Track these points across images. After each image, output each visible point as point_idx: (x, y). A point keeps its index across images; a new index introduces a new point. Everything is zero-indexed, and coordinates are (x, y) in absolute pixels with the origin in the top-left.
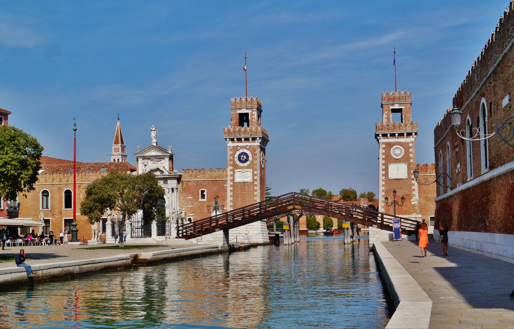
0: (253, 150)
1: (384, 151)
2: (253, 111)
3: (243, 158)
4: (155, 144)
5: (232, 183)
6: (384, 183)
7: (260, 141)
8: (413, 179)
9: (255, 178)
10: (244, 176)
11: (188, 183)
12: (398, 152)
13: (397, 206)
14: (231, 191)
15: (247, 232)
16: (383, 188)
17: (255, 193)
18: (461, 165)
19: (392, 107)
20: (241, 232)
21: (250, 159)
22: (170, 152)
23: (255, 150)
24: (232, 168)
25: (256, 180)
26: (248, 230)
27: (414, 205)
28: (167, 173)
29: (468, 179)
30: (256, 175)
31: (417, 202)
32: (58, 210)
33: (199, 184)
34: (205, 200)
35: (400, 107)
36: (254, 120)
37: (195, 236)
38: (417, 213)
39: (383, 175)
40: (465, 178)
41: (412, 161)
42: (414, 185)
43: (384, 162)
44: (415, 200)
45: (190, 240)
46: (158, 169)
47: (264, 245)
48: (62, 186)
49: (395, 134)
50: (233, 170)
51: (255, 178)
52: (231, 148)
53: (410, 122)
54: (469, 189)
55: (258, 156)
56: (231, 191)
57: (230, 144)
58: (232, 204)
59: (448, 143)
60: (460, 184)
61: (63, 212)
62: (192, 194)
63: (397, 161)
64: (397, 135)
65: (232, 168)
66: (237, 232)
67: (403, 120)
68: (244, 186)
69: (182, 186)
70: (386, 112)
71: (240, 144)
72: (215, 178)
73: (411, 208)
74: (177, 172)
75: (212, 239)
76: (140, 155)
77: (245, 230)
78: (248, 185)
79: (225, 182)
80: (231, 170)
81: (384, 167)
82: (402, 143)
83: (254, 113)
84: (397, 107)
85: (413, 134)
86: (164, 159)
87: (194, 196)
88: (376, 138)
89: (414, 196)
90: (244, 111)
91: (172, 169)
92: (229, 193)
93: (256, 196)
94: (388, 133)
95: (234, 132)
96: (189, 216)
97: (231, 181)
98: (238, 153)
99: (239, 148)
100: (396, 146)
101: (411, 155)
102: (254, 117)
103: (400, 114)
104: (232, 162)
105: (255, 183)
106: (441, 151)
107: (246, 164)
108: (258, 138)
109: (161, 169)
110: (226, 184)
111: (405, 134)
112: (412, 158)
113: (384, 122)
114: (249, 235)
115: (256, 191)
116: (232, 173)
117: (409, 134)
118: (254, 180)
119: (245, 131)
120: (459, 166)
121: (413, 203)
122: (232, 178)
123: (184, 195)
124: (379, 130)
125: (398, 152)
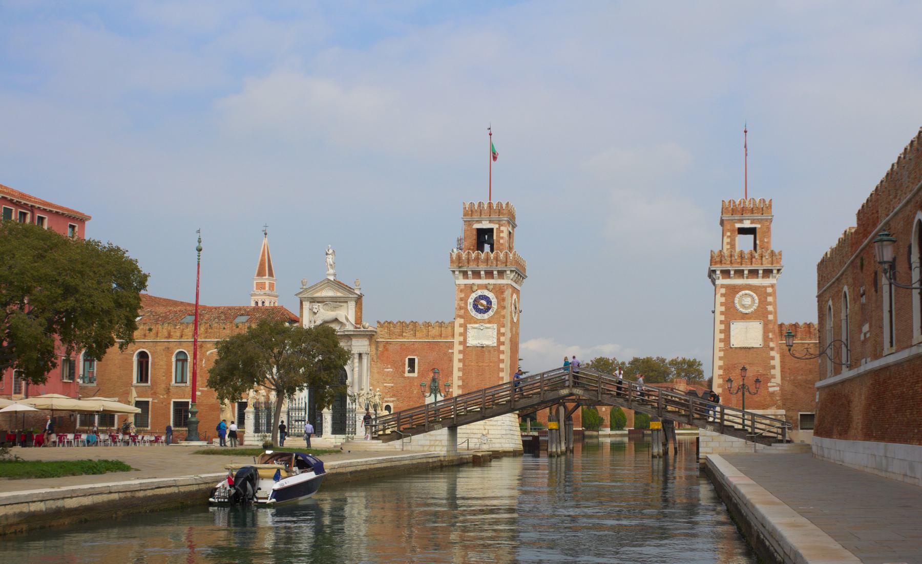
0: (499, 291)
1: (723, 300)
2: (500, 225)
3: (482, 305)
4: (332, 278)
5: (461, 348)
6: (722, 354)
7: (512, 276)
8: (772, 349)
9: (502, 339)
10: (482, 335)
12: (747, 301)
13: (747, 394)
14: (460, 360)
16: (721, 363)
17: (501, 366)
18: (870, 327)
19: (738, 225)
20: (475, 431)
21: (495, 306)
22: (358, 292)
23: (502, 293)
24: (462, 321)
25: (503, 343)
26: (487, 427)
27: (773, 393)
28: (352, 328)
29: (886, 352)
30: (503, 334)
31: (778, 389)
33: (405, 348)
34: (415, 375)
35: (753, 226)
36: (501, 241)
37: (399, 437)
38: (779, 408)
39: (721, 340)
40: (879, 349)
41: (771, 317)
42: (773, 358)
43: (723, 318)
44: (775, 385)
45: (391, 443)
46: (336, 320)
47: (514, 454)
48: (171, 345)
49: (743, 271)
50: (464, 326)
51: (502, 339)
52: (462, 287)
53: (769, 251)
54: (886, 368)
55: (507, 303)
56: (460, 360)
57: (461, 281)
58: (460, 383)
59: (846, 288)
60: (869, 359)
61: (172, 390)
62: (394, 364)
63: (745, 317)
64: (746, 272)
65: (462, 321)
66: (469, 431)
67: (758, 248)
68: (483, 352)
69: (377, 350)
70: (729, 234)
71: (477, 282)
73: (769, 399)
74: (369, 324)
75: (428, 443)
76: (305, 296)
77: (482, 427)
78: (489, 351)
79: (451, 345)
80: (461, 326)
81: (722, 327)
82: (755, 286)
83: (502, 228)
84: (747, 224)
85: (775, 272)
88: (710, 276)
89: (774, 377)
90: (485, 225)
91: (359, 320)
92: (457, 365)
93: (502, 370)
94: (732, 269)
95: (468, 261)
96: (386, 402)
97: (460, 343)
98: (474, 296)
99: (475, 288)
100: (743, 292)
101: (770, 308)
102: (502, 235)
103: (752, 236)
105: (502, 348)
106: (830, 302)
107: (486, 316)
108: (508, 272)
109: (340, 320)
111: (761, 272)
112: (770, 313)
113: (725, 250)
114: (489, 436)
115: (503, 361)
116: (462, 330)
117: (768, 273)
118: (500, 343)
119: (487, 260)
120: (866, 328)
121: (771, 389)
122: (461, 339)
123: (379, 365)
124: (716, 263)
125: (747, 301)
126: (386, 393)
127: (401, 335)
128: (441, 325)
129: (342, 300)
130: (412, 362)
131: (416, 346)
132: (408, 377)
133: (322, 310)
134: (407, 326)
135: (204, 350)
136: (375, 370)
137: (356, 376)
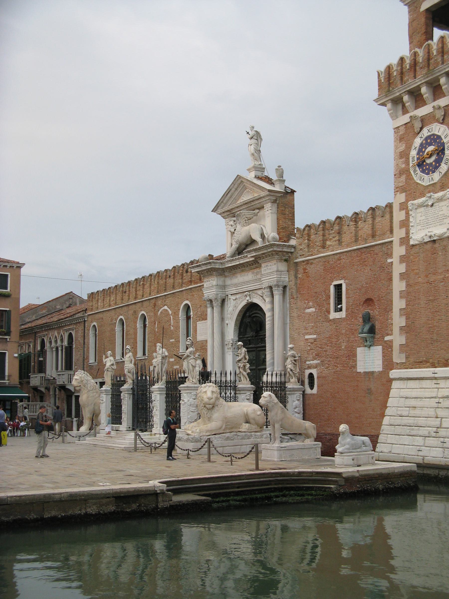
15: (437, 422)
20: (421, 421)
22: (277, 188)
24: (402, 197)
26: (441, 413)
33: (332, 267)
34: (343, 314)
52: (402, 131)
56: (402, 276)
66: (411, 421)
68: (434, 252)
69: (296, 277)
72: (366, 240)
87: (319, 305)
92: (398, 286)
96: (309, 367)
98: (418, 141)
104: (403, 178)
107: (436, 177)
110: (390, 255)
114: (442, 432)
122: (402, 233)
133: (239, 227)
135: (157, 308)
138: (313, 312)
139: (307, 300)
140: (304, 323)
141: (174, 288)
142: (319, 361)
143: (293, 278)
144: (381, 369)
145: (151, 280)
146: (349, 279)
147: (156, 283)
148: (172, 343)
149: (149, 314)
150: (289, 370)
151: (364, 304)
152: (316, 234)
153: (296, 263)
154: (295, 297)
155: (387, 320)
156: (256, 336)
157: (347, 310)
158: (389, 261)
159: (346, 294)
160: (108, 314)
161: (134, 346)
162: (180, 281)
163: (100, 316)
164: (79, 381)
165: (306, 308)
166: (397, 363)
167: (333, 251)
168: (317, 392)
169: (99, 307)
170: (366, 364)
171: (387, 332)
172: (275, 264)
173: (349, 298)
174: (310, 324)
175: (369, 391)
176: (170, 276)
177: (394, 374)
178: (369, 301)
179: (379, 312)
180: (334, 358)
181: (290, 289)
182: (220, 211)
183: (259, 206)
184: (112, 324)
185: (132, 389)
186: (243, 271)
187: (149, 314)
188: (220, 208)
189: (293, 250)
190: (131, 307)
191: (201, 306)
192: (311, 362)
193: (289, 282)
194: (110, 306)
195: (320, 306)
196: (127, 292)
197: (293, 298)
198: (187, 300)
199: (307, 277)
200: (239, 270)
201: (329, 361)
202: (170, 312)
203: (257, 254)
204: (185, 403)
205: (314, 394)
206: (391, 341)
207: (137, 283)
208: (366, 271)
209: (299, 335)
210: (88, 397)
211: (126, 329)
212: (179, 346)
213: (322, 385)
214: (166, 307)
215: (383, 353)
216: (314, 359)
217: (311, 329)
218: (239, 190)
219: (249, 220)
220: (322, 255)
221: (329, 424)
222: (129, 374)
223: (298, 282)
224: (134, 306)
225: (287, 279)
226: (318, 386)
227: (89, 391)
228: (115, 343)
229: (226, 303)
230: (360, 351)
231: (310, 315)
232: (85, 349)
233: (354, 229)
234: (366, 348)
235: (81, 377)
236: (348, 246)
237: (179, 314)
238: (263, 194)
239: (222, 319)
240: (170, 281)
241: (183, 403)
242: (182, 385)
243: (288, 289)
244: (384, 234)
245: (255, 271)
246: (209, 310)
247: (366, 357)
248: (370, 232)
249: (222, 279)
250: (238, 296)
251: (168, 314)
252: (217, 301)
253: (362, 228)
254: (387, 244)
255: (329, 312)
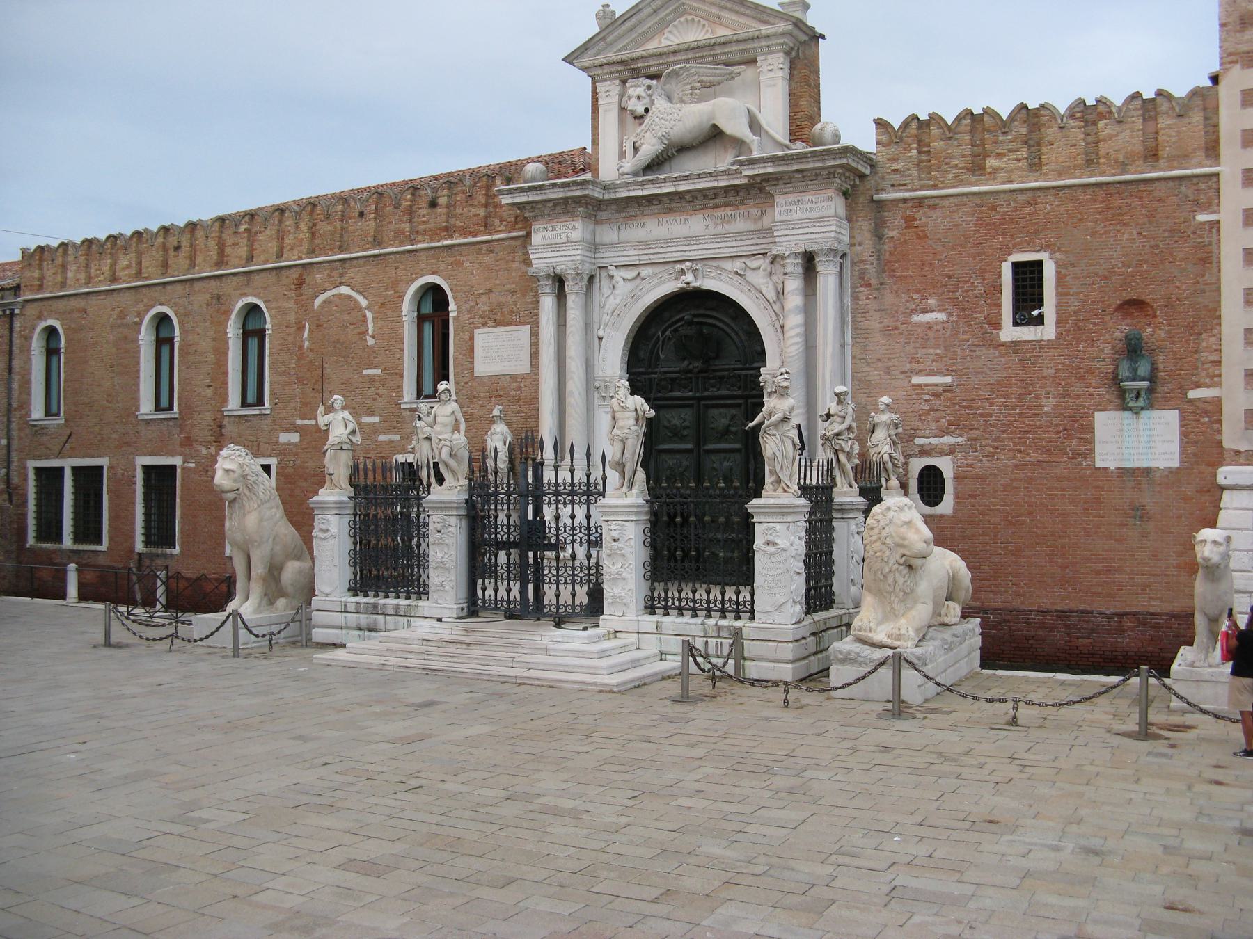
11: (922, 216)
32: (209, 417)
33: (997, 222)
34: (1048, 331)
48: (228, 286)
61: (230, 428)
69: (879, 236)
72: (1123, 167)
86: (753, 61)
96: (924, 452)
123: (889, 299)
126: (922, 416)
127: (976, 167)
128: (1149, 107)
129: (735, 51)
130: (1028, 276)
131: (1045, 209)
132: (1015, 344)
133: (660, 104)
134: (1004, 126)
135: (307, 291)
136: (874, 323)
137: (794, 346)
138: (937, 322)
139: (918, 292)
140: (909, 347)
141: (378, 243)
142: (960, 439)
143: (866, 236)
144: (1176, 463)
145: (280, 222)
146: (1066, 252)
147: (303, 227)
148: (372, 379)
149: (274, 304)
150: (886, 457)
151: (1116, 310)
152: (950, 138)
153: (880, 202)
154: (874, 282)
155: (1196, 352)
156: (701, 371)
157: (1060, 322)
158: (1202, 218)
159: (1057, 287)
160: (108, 301)
161: (212, 380)
162: (406, 227)
163: (73, 303)
164: (236, 475)
165: (914, 311)
166: (1238, 453)
167: (1011, 182)
168: (955, 511)
169: (69, 282)
170: (1125, 451)
171: (1194, 378)
172: (829, 199)
173: (1067, 294)
174: (931, 351)
175: (1141, 514)
176: (361, 215)
177: (1227, 474)
178: (1134, 306)
179: (1168, 332)
180: (1013, 433)
181: (853, 264)
182: (588, 60)
183: (738, 57)
184: (127, 326)
185: (467, 502)
186: (670, 211)
187: (274, 304)
188: (591, 52)
189: (868, 172)
190: (198, 286)
191: (491, 290)
192: (934, 440)
193: (852, 245)
194: (114, 279)
195: (963, 310)
196: (185, 250)
197: (869, 285)
198: (434, 273)
199: (919, 238)
200: (656, 208)
201: (996, 440)
202: (364, 303)
203: (780, 169)
204: (783, 550)
205: (942, 516)
206: (1218, 402)
207: (222, 226)
208: (1126, 236)
209: (888, 374)
210: (261, 520)
211: (182, 340)
212: (400, 387)
213: (973, 496)
214: (345, 290)
215: (1181, 426)
216: (943, 432)
217: (933, 361)
218: (662, 14)
219: (708, 89)
220: (975, 189)
221: (997, 586)
222: (452, 463)
223: (887, 247)
224: (213, 283)
225: (847, 239)
226: (957, 497)
227: (263, 502)
228: (138, 372)
229: (596, 286)
230: (1101, 418)
231: (930, 328)
232: (15, 385)
233: (1082, 136)
234: (1127, 414)
235: (241, 466)
236: (1060, 175)
237: (398, 309)
238: (765, 29)
239: (587, 326)
240: (369, 225)
241: (771, 549)
242: (755, 501)
243: (848, 263)
244: (1186, 156)
245: (719, 213)
246: (548, 302)
247: (1126, 434)
248: (1139, 148)
249: (591, 227)
250: (645, 272)
251: (357, 306)
252: (581, 280)
253: (1111, 137)
254: (1195, 181)
255: (997, 325)
